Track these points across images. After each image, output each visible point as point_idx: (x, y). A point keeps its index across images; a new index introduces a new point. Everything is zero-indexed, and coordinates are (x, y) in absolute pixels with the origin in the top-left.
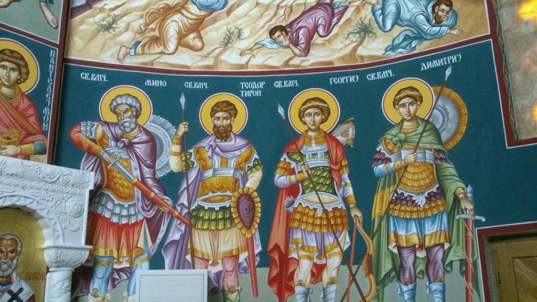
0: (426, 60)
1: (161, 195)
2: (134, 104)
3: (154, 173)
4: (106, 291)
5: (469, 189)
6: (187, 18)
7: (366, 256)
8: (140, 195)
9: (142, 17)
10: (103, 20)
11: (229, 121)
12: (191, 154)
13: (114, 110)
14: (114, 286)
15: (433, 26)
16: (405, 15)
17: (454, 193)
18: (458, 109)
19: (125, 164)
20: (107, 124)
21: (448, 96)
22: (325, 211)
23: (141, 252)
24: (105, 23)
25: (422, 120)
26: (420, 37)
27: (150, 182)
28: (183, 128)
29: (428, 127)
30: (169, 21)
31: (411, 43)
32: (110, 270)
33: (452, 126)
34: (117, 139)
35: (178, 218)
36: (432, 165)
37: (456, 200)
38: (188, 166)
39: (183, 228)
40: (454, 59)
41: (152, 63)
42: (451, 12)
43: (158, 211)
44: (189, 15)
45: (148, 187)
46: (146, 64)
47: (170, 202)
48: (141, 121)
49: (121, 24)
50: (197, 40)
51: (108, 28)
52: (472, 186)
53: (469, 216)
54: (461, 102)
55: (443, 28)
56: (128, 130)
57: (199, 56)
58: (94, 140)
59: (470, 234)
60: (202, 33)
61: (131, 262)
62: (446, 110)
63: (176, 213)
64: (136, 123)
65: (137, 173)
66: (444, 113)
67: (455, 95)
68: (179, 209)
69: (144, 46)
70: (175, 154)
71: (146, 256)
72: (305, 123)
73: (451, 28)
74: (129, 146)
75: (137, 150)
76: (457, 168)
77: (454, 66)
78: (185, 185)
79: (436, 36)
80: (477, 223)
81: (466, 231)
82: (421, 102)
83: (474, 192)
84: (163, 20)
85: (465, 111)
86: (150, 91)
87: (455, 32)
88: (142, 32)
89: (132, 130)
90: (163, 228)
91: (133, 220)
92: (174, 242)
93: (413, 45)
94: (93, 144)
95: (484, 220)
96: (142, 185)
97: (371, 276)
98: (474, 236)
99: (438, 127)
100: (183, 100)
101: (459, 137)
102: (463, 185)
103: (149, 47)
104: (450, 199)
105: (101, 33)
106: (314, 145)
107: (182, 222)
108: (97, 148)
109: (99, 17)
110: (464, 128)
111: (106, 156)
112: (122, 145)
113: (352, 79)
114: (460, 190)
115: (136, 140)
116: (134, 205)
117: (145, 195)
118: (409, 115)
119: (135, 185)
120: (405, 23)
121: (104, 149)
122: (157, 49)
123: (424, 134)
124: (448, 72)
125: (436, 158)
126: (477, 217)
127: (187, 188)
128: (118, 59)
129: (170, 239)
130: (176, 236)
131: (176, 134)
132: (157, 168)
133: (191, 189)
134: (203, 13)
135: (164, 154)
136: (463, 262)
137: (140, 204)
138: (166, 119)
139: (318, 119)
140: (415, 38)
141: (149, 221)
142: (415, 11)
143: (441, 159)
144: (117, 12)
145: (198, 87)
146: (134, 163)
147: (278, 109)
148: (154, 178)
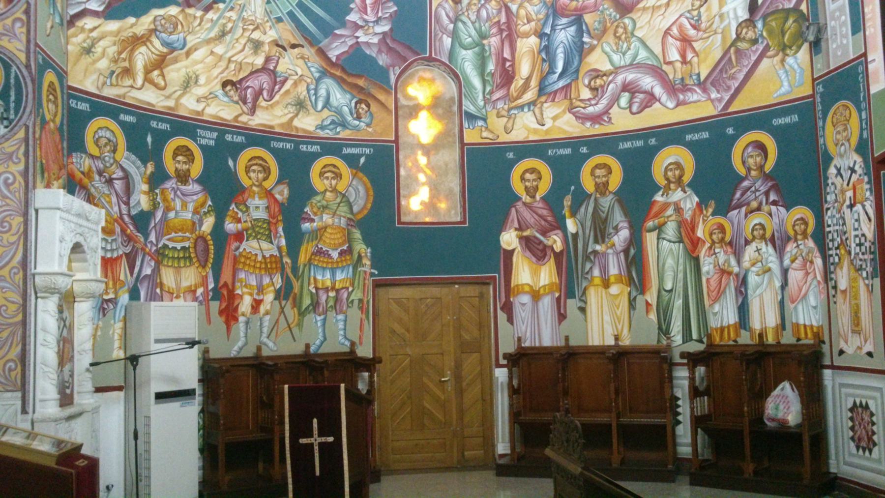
0: (347, 146)
1: (135, 232)
2: (112, 138)
3: (129, 211)
4: (99, 319)
5: (369, 250)
6: (152, 53)
7: (292, 294)
8: (119, 230)
9: (115, 44)
10: (84, 41)
11: (187, 166)
12: (157, 194)
13: (96, 142)
14: (104, 315)
15: (354, 119)
16: (334, 101)
17: (359, 252)
18: (367, 191)
19: (107, 199)
20: (92, 157)
21: (361, 179)
22: (264, 257)
23: (123, 284)
24: (85, 45)
25: (341, 193)
26: (344, 125)
27: (126, 219)
28: (150, 168)
29: (344, 200)
30: (137, 52)
31: (336, 128)
32: (101, 300)
33: (361, 202)
34: (100, 173)
35: (150, 255)
36: (345, 229)
37: (360, 257)
38: (155, 206)
39: (153, 263)
40: (368, 151)
41: (124, 96)
42: (368, 113)
43: (134, 247)
44: (153, 50)
45: (126, 224)
46: (119, 96)
47: (142, 240)
48: (118, 156)
49: (98, 49)
50: (160, 78)
51: (88, 51)
52: (372, 248)
53: (367, 269)
54: (369, 185)
55: (362, 124)
56: (108, 165)
57: (163, 95)
58: (83, 173)
59: (367, 282)
60: (165, 71)
61: (116, 293)
62: (358, 189)
63: (147, 250)
64: (114, 158)
65: (116, 209)
66: (357, 191)
67: (365, 179)
68: (149, 246)
69: (118, 75)
70: (145, 193)
71: (126, 288)
72: (250, 178)
73: (368, 125)
74: (110, 182)
75: (116, 186)
76: (362, 234)
77: (367, 156)
78: (153, 225)
79: (356, 128)
80: (372, 275)
81: (365, 279)
82: (341, 178)
83: (372, 253)
84: (132, 51)
85: (371, 193)
86: (123, 125)
87: (370, 130)
88: (116, 61)
89: (112, 165)
90: (138, 263)
91: (115, 255)
92: (146, 276)
93: (338, 130)
94: (82, 176)
95: (376, 273)
96: (120, 220)
97: (295, 309)
98: (369, 283)
99: (351, 200)
100: (149, 139)
101: (366, 212)
102: (364, 246)
103: (122, 78)
104: (356, 256)
105: (83, 56)
106: (257, 199)
107: (152, 258)
108: (86, 181)
109: (81, 37)
110: (369, 206)
111: (93, 190)
112: (103, 180)
113: (288, 146)
114: (363, 250)
115: (114, 176)
116: (115, 240)
117: (123, 231)
118: (331, 187)
119: (116, 221)
120: (333, 109)
121: (91, 183)
122: (128, 82)
123: (341, 205)
124: (362, 160)
125: (348, 225)
126: (373, 271)
127: (155, 226)
128: (98, 88)
129: (143, 274)
130: (148, 271)
131: (145, 173)
132: (131, 206)
133: (158, 228)
134: (165, 50)
135: (136, 193)
136: (361, 301)
137: (120, 240)
138: (137, 157)
139: (261, 176)
140: (340, 125)
141: (127, 255)
142: (342, 101)
143: (352, 225)
144: (94, 34)
145: (162, 128)
146: (114, 199)
147: (228, 163)
148: (129, 215)
